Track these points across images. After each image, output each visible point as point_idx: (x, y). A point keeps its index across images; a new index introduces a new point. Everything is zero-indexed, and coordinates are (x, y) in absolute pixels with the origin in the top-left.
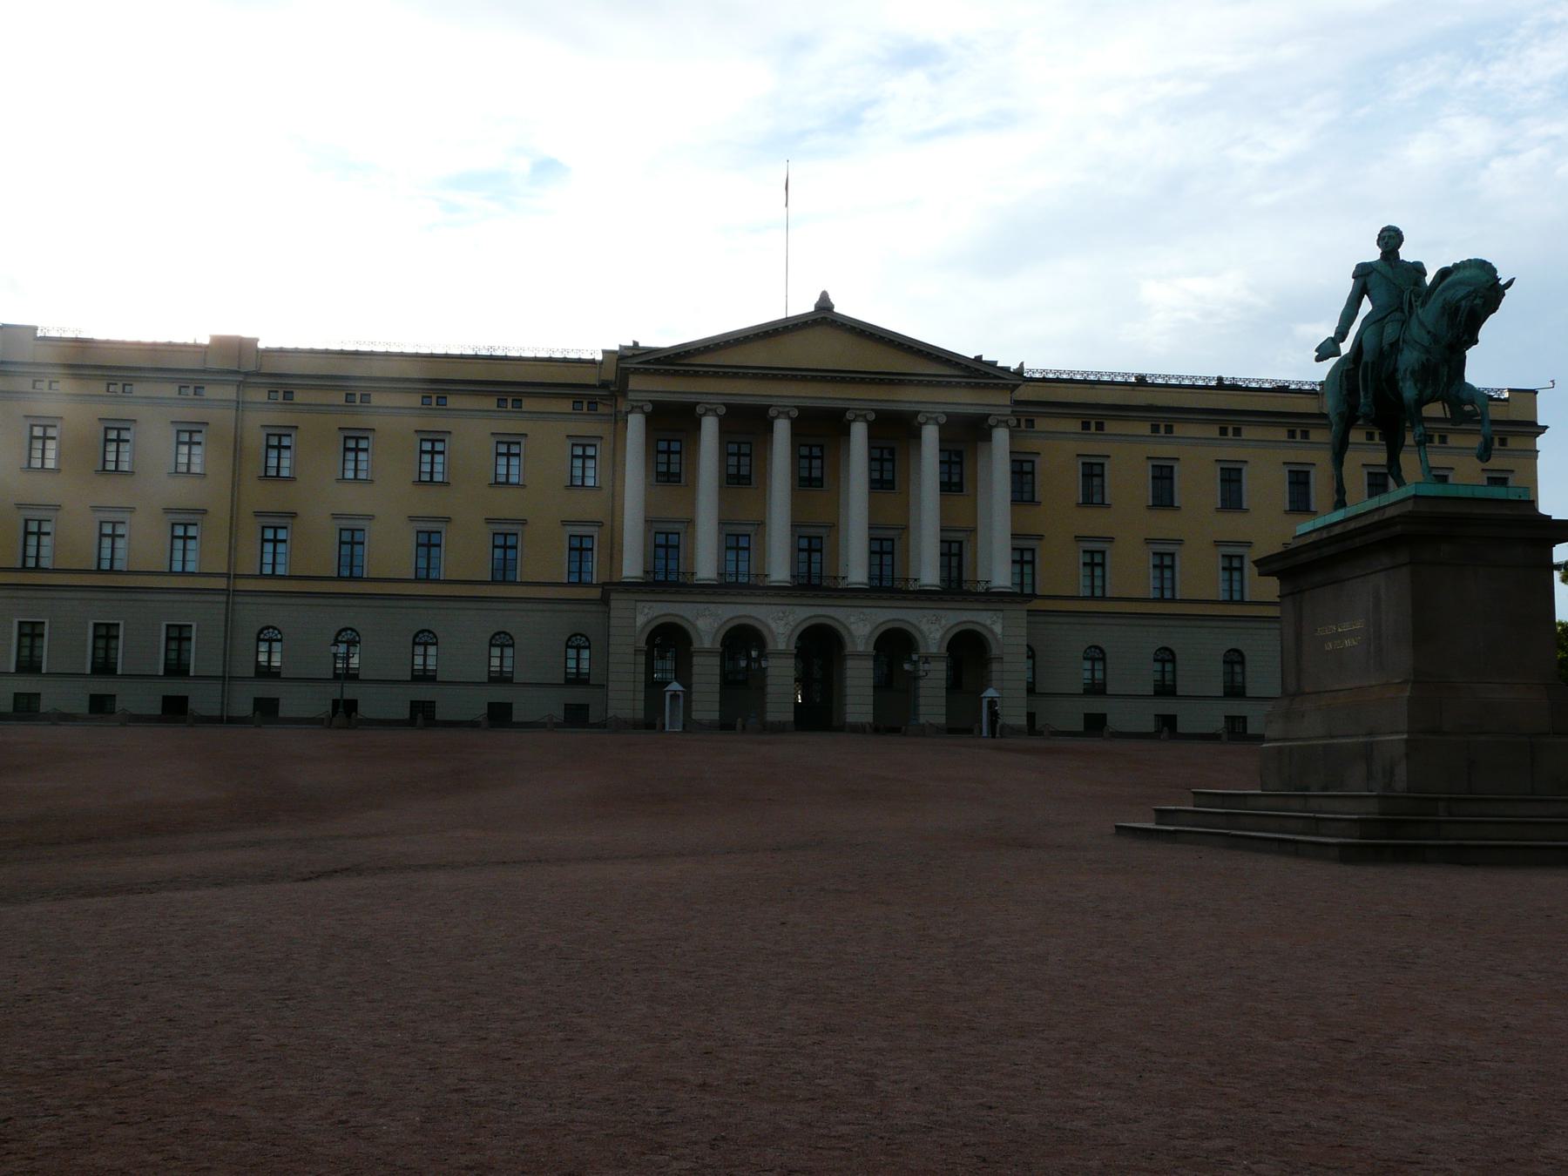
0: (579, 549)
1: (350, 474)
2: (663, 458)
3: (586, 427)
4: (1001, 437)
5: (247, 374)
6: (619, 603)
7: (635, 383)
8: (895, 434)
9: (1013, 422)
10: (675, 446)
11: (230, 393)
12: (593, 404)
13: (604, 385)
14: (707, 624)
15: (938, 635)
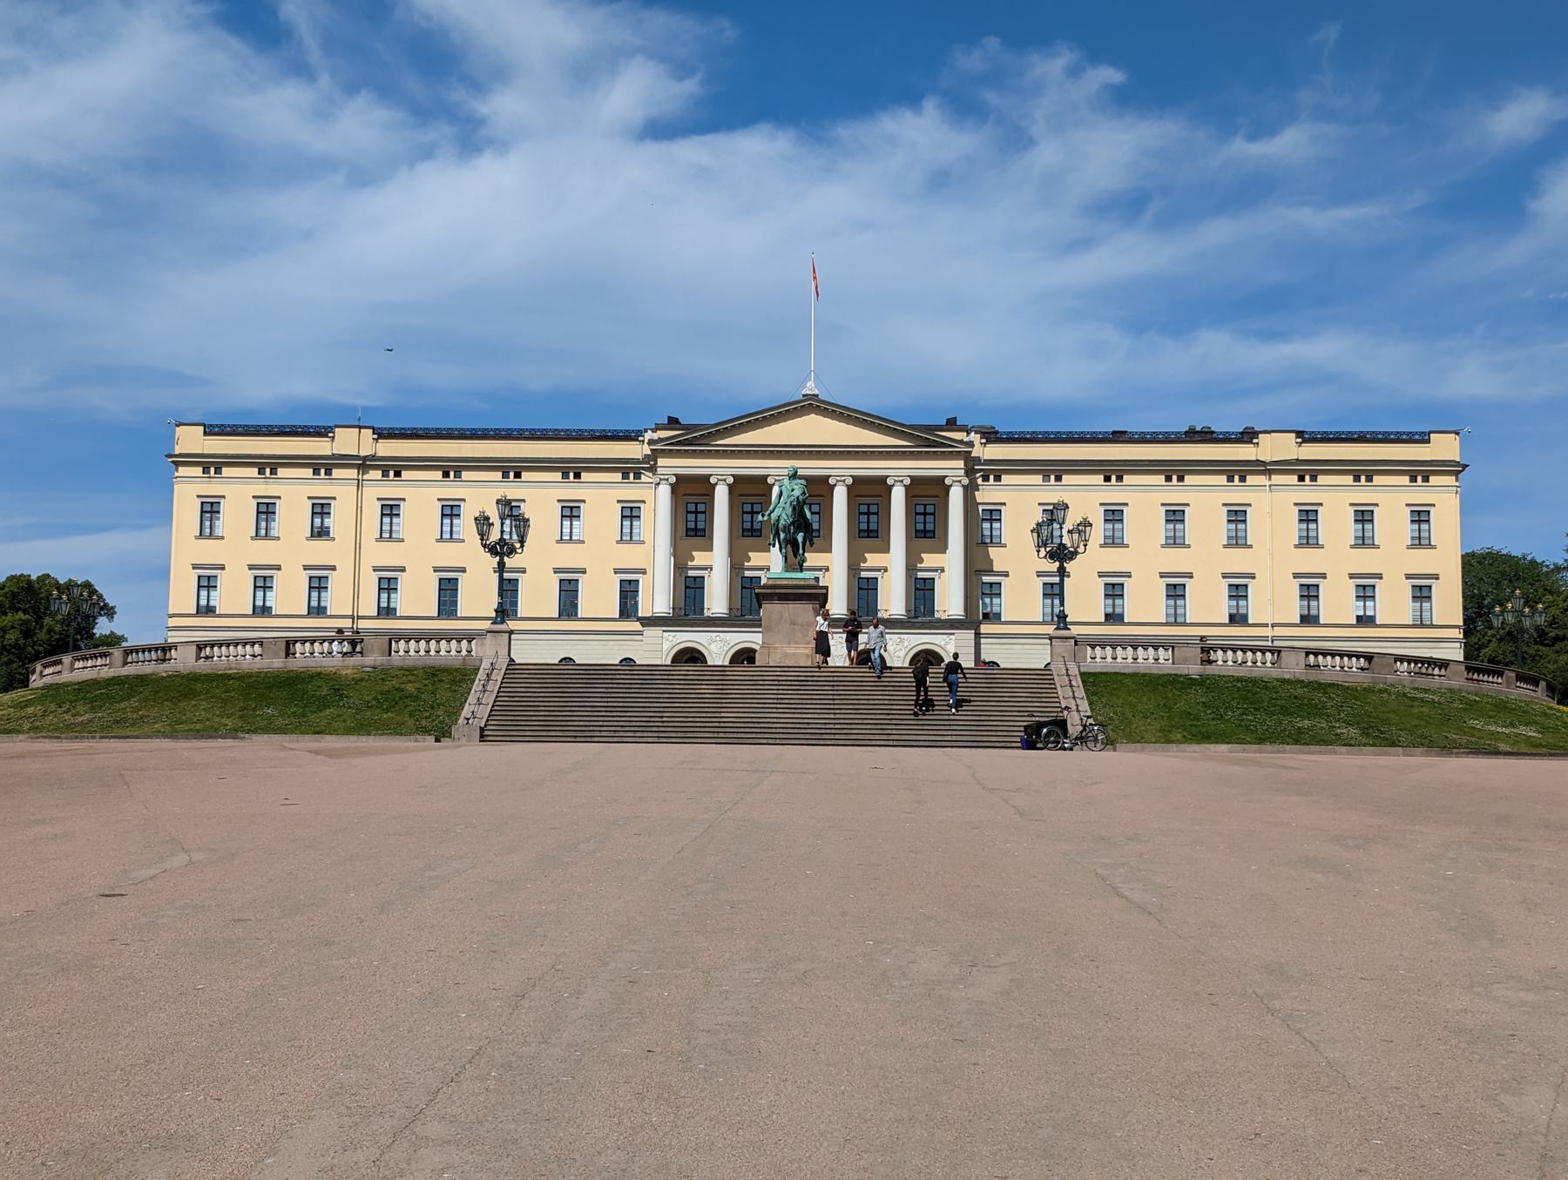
0: (628, 592)
1: (447, 536)
2: (691, 517)
3: (631, 492)
4: (956, 497)
5: (365, 458)
6: (653, 633)
7: (660, 462)
8: (869, 496)
9: (966, 481)
10: (701, 508)
11: (353, 473)
12: (637, 476)
13: (647, 458)
14: (718, 647)
15: (902, 654)
